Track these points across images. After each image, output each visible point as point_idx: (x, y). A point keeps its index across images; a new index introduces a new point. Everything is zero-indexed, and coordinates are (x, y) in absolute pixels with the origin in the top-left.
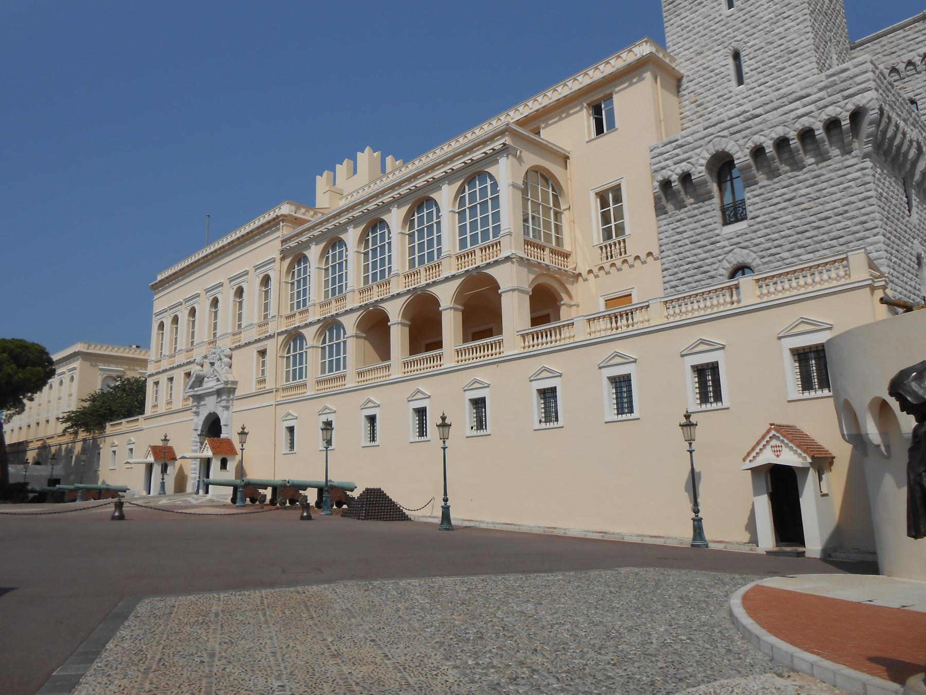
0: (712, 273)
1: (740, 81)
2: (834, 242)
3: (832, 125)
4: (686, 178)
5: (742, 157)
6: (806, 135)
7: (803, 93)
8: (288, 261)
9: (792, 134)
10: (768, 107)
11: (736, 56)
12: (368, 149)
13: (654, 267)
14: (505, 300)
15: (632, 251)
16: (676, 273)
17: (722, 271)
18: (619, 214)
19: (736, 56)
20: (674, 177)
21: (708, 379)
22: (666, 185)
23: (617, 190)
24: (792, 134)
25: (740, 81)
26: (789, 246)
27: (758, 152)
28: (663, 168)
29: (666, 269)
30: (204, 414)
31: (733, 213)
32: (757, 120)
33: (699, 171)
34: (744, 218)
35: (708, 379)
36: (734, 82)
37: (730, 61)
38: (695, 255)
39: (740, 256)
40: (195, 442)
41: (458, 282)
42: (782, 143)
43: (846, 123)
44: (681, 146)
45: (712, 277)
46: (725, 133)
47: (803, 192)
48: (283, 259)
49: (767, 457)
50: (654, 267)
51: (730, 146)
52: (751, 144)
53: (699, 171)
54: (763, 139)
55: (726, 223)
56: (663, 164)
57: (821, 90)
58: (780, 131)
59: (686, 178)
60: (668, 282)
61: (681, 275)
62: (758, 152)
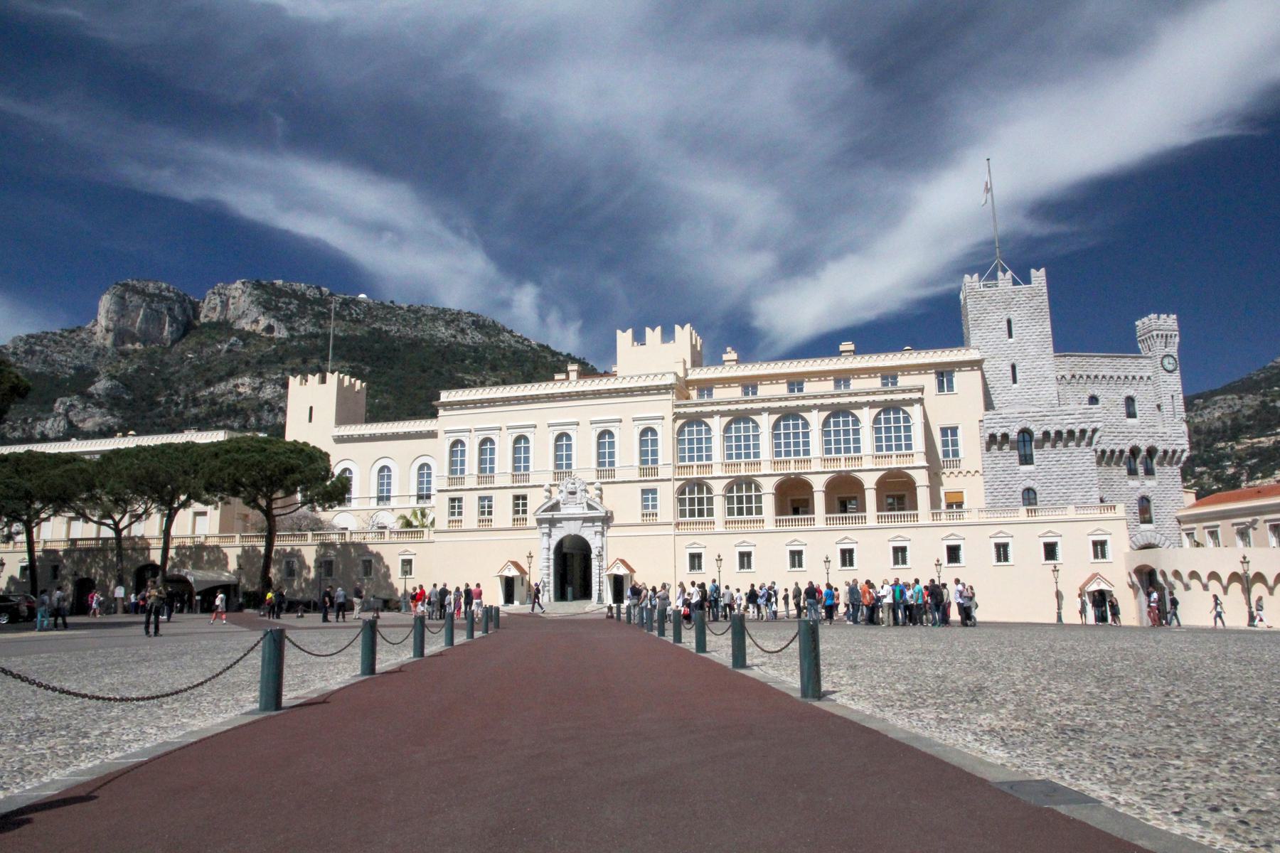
1: (1015, 381)
3: (1083, 432)
4: (1005, 436)
5: (1038, 434)
6: (1071, 433)
8: (680, 422)
9: (1065, 431)
11: (1013, 367)
12: (688, 326)
13: (979, 479)
14: (919, 490)
15: (964, 466)
18: (955, 443)
19: (1013, 367)
21: (1050, 551)
22: (993, 436)
23: (954, 430)
24: (1065, 431)
25: (1015, 381)
27: (1046, 434)
30: (558, 534)
31: (1026, 459)
33: (1013, 435)
34: (1032, 463)
35: (1050, 551)
37: (1010, 368)
39: (1029, 484)
41: (882, 473)
42: (1059, 433)
43: (1089, 434)
48: (675, 420)
49: (1094, 587)
50: (979, 479)
51: (1032, 427)
52: (1043, 429)
53: (1013, 435)
55: (1021, 464)
58: (1058, 427)
59: (1005, 436)
62: (1046, 434)
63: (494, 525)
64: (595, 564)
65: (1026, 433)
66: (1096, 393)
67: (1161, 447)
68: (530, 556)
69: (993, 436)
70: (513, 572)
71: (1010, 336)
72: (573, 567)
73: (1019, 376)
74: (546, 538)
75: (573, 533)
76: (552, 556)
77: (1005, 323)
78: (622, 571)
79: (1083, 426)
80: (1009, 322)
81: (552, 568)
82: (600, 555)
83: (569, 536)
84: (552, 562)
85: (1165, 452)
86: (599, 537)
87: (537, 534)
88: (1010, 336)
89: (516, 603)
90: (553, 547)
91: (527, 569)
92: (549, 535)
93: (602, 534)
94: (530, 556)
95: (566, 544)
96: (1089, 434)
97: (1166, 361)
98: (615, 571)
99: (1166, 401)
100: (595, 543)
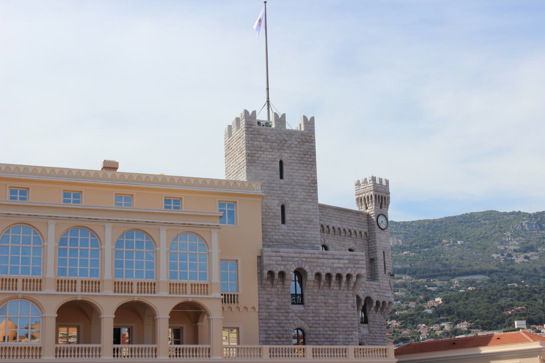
0: (287, 328)
1: (283, 222)
2: (341, 329)
3: (349, 276)
4: (282, 274)
5: (311, 276)
6: (339, 276)
7: (340, 257)
10: (325, 256)
11: (283, 207)
16: (267, 323)
17: (291, 329)
19: (283, 207)
20: (277, 272)
25: (283, 222)
26: (322, 325)
27: (318, 275)
28: (271, 264)
29: (262, 319)
32: (320, 261)
36: (280, 221)
37: (280, 208)
38: (278, 316)
42: (329, 275)
44: (282, 257)
45: (286, 331)
46: (304, 260)
47: (330, 301)
51: (306, 268)
52: (316, 271)
54: (321, 271)
55: (293, 304)
56: (272, 262)
57: (347, 259)
58: (329, 270)
59: (282, 274)
60: (262, 327)
61: (270, 325)
62: (318, 275)
65: (300, 274)
66: (327, 242)
67: (375, 297)
69: (271, 273)
71: (281, 177)
73: (288, 217)
77: (278, 163)
79: (349, 271)
80: (281, 163)
85: (378, 302)
88: (281, 177)
96: (354, 279)
97: (380, 222)
99: (380, 255)
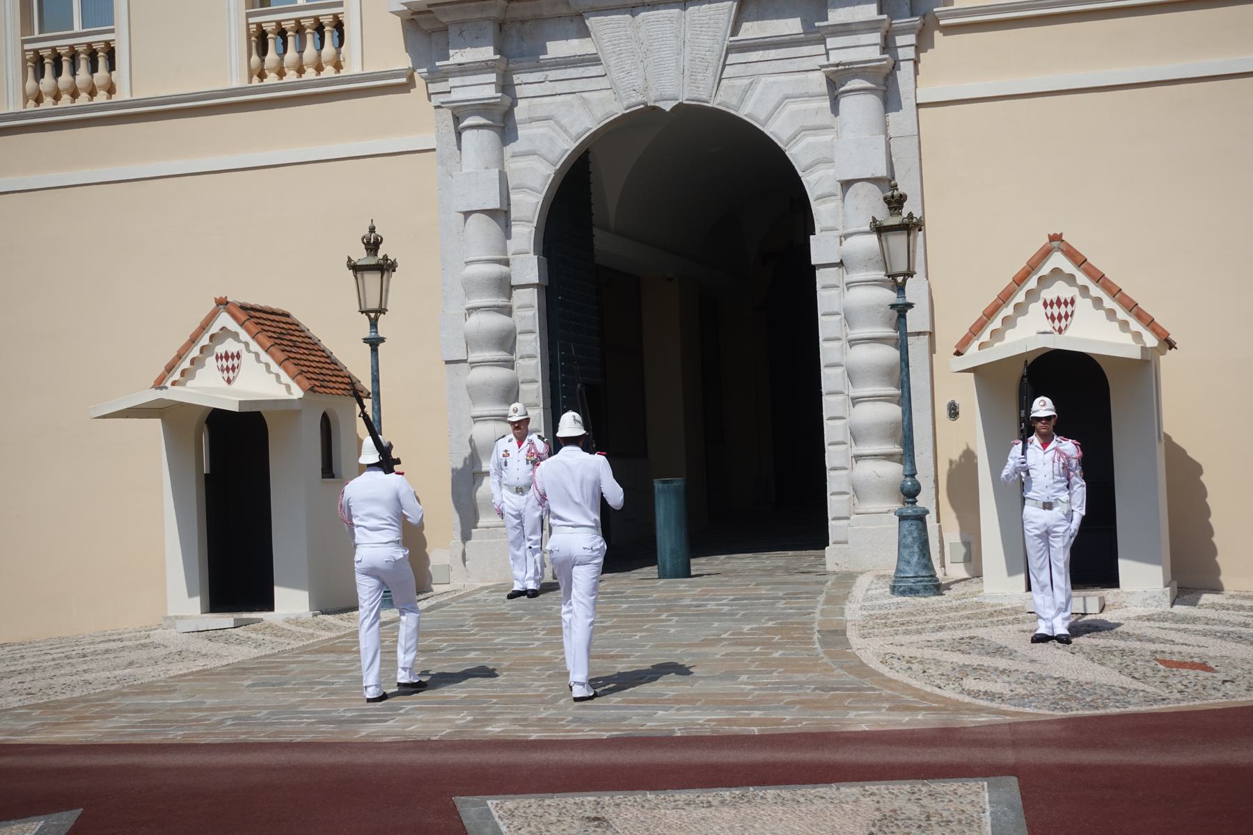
30: (564, 111)
40: (470, 286)
63: (131, 83)
64: (846, 306)
68: (375, 263)
70: (260, 382)
72: (688, 328)
74: (478, 142)
75: (670, 88)
76: (528, 269)
78: (1094, 333)
81: (530, 345)
82: (899, 222)
83: (640, 124)
84: (527, 310)
86: (859, 106)
87: (416, 120)
89: (291, 602)
90: (529, 205)
91: (356, 363)
92: (502, 122)
93: (889, 97)
94: (375, 263)
95: (609, 192)
98: (1029, 334)
100: (832, 151)
